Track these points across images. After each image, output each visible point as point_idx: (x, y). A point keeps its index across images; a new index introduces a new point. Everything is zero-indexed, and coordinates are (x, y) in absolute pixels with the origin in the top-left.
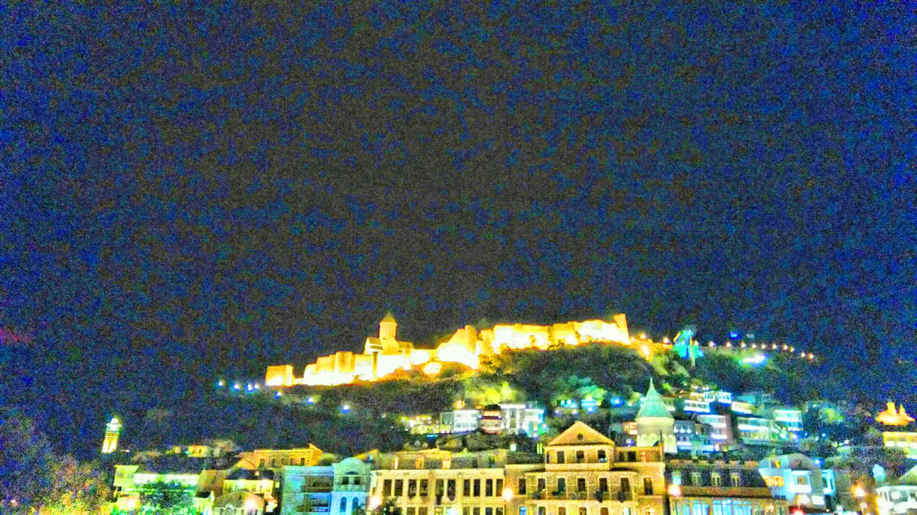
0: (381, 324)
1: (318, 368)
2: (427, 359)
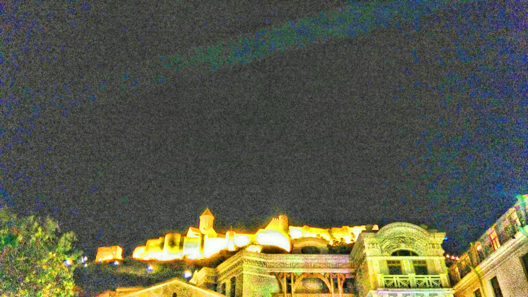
0: (201, 217)
1: (147, 250)
2: (249, 244)
